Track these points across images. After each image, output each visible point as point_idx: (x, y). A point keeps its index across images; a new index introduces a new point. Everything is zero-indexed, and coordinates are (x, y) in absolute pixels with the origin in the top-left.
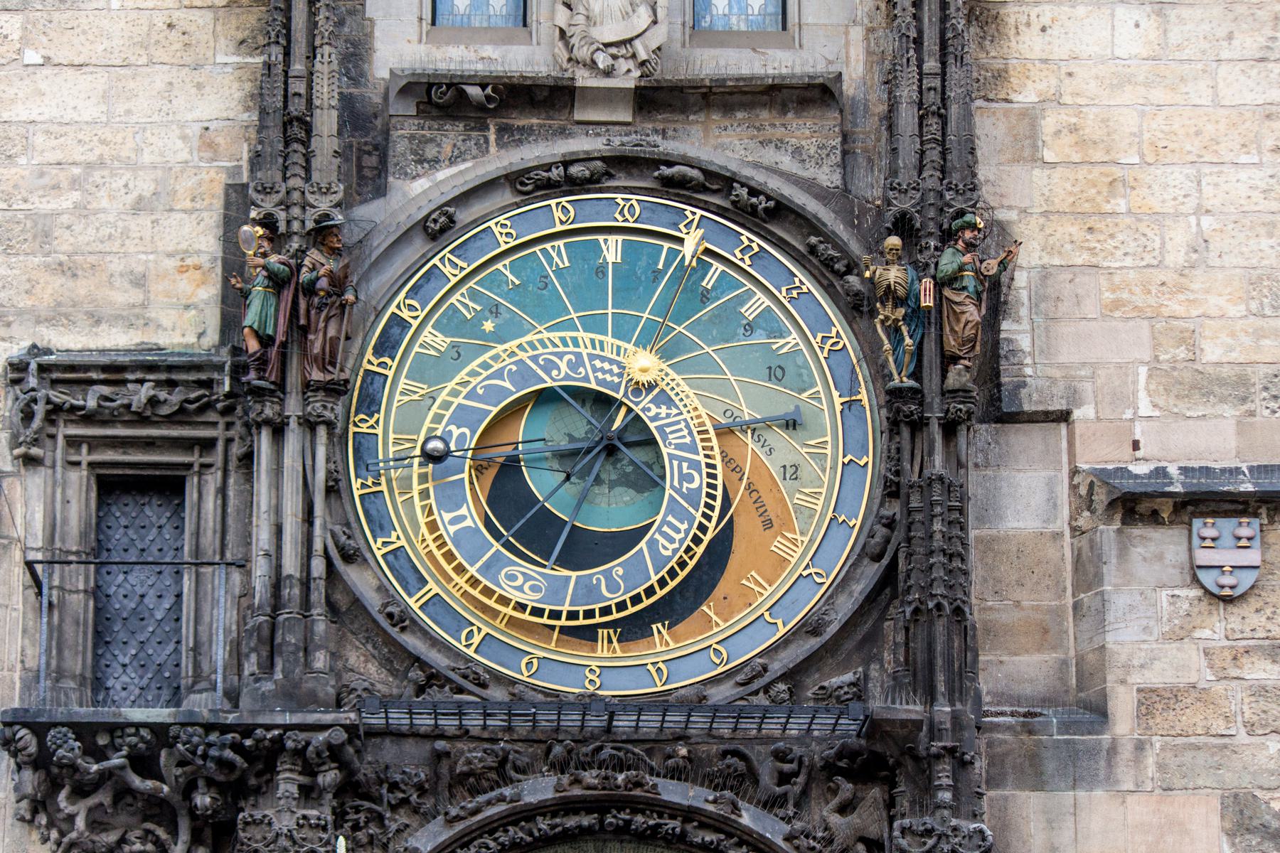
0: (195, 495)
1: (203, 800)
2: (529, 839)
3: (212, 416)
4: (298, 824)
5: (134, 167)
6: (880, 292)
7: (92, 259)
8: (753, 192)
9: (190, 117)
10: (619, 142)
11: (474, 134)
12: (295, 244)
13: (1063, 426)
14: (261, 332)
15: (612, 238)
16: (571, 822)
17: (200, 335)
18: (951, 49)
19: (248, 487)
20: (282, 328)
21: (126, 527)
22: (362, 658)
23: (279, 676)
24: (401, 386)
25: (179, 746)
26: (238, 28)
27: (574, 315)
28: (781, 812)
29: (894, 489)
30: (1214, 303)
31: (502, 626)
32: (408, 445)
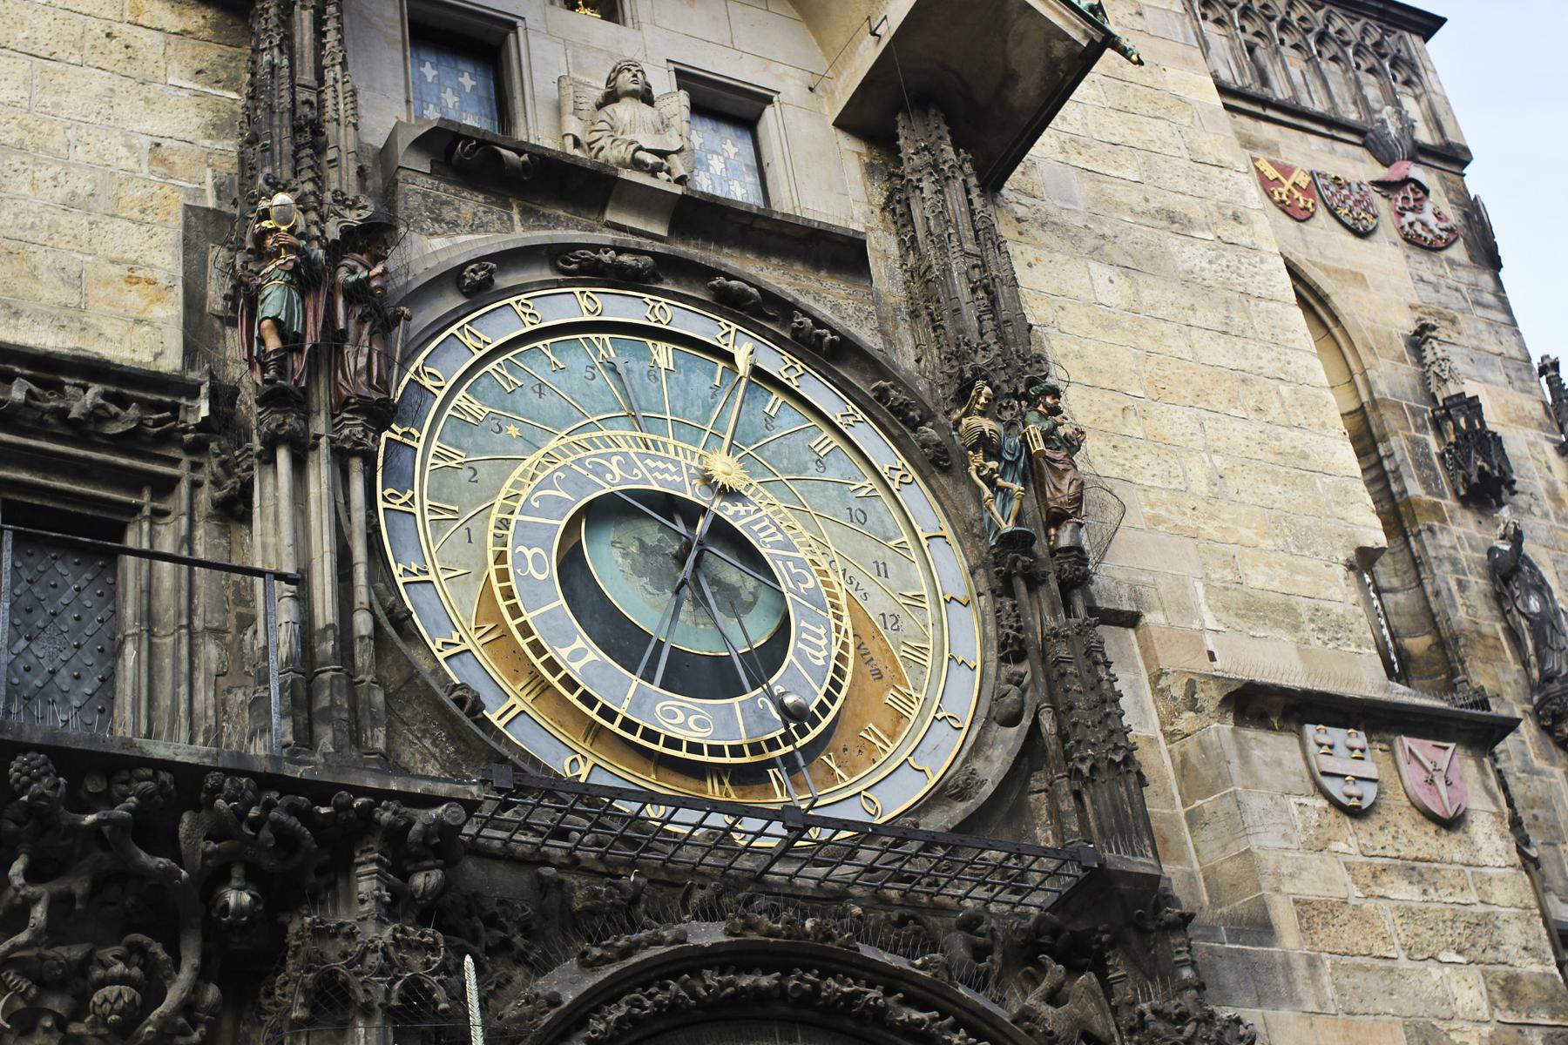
3: (175, 453)
5: (67, 165)
7: (11, 245)
8: (818, 323)
9: (136, 128)
10: (659, 247)
11: (496, 209)
13: (1131, 632)
15: (662, 346)
16: (746, 981)
17: (157, 356)
19: (224, 542)
21: (30, 582)
22: (418, 757)
24: (433, 449)
25: (220, 803)
26: (194, 58)
29: (1016, 648)
30: (1247, 534)
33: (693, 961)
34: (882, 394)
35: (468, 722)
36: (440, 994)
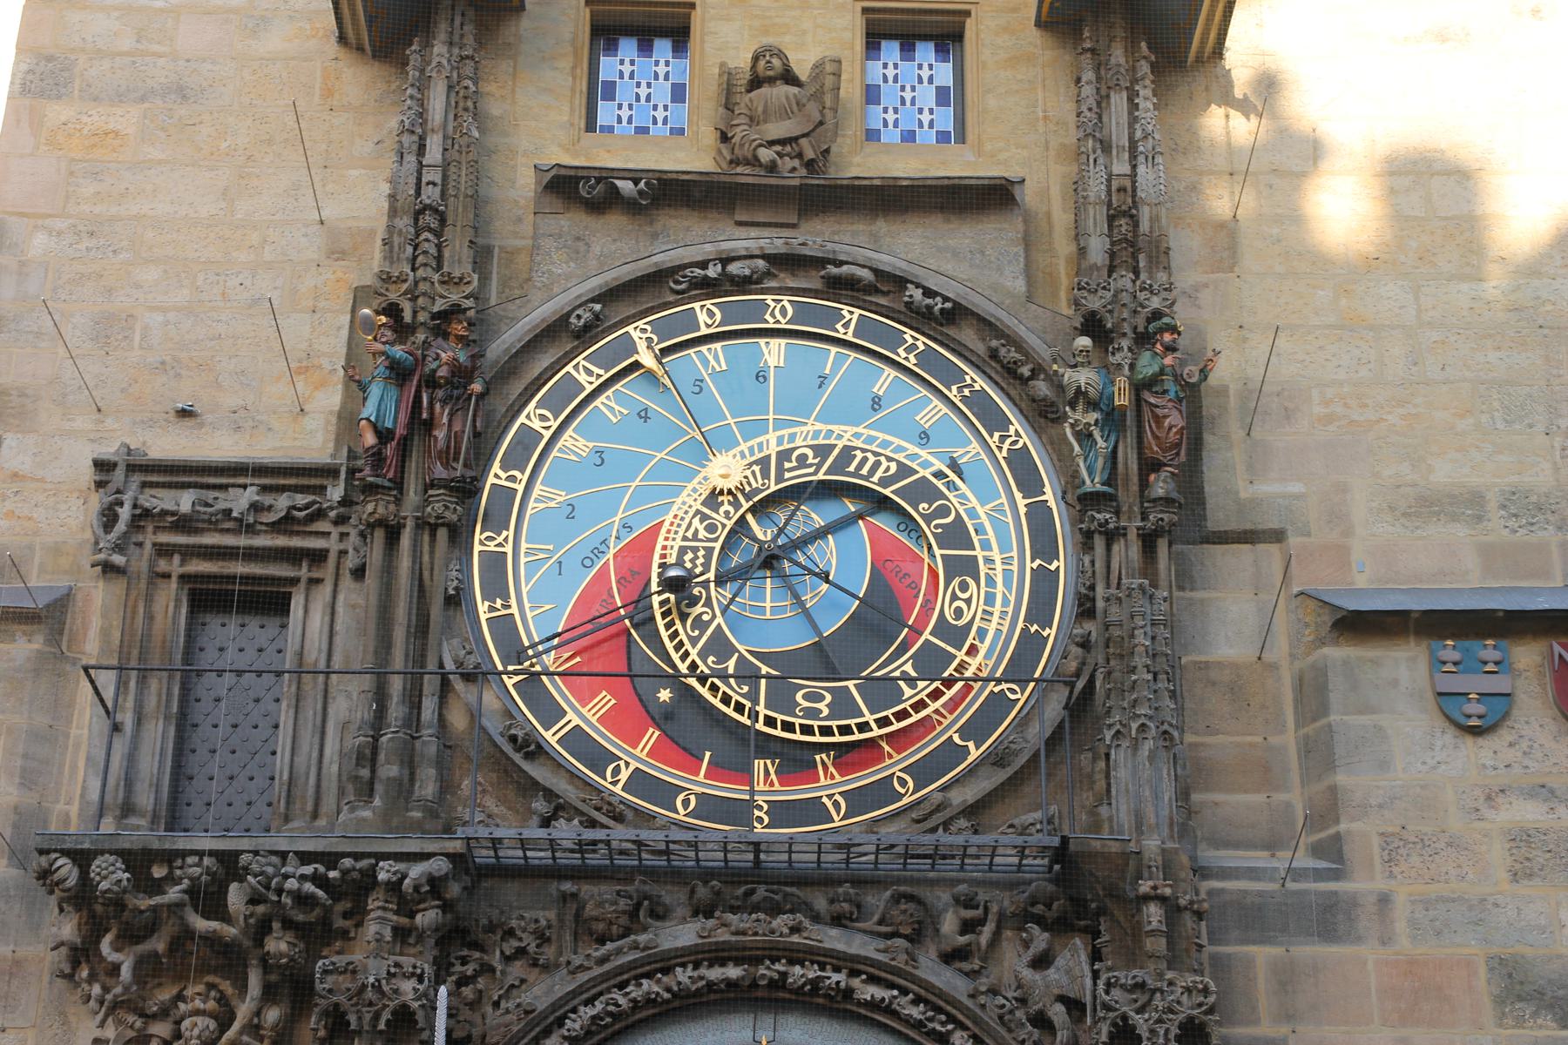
0: (301, 612)
1: (279, 944)
2: (667, 996)
4: (388, 972)
6: (1071, 393)
8: (928, 293)
12: (421, 336)
14: (379, 425)
16: (715, 974)
18: (1141, 149)
20: (403, 418)
23: (377, 802)
27: (731, 421)
28: (966, 966)
31: (643, 756)
32: (542, 556)
33: (665, 963)
34: (994, 354)
35: (517, 758)
36: (420, 1016)
